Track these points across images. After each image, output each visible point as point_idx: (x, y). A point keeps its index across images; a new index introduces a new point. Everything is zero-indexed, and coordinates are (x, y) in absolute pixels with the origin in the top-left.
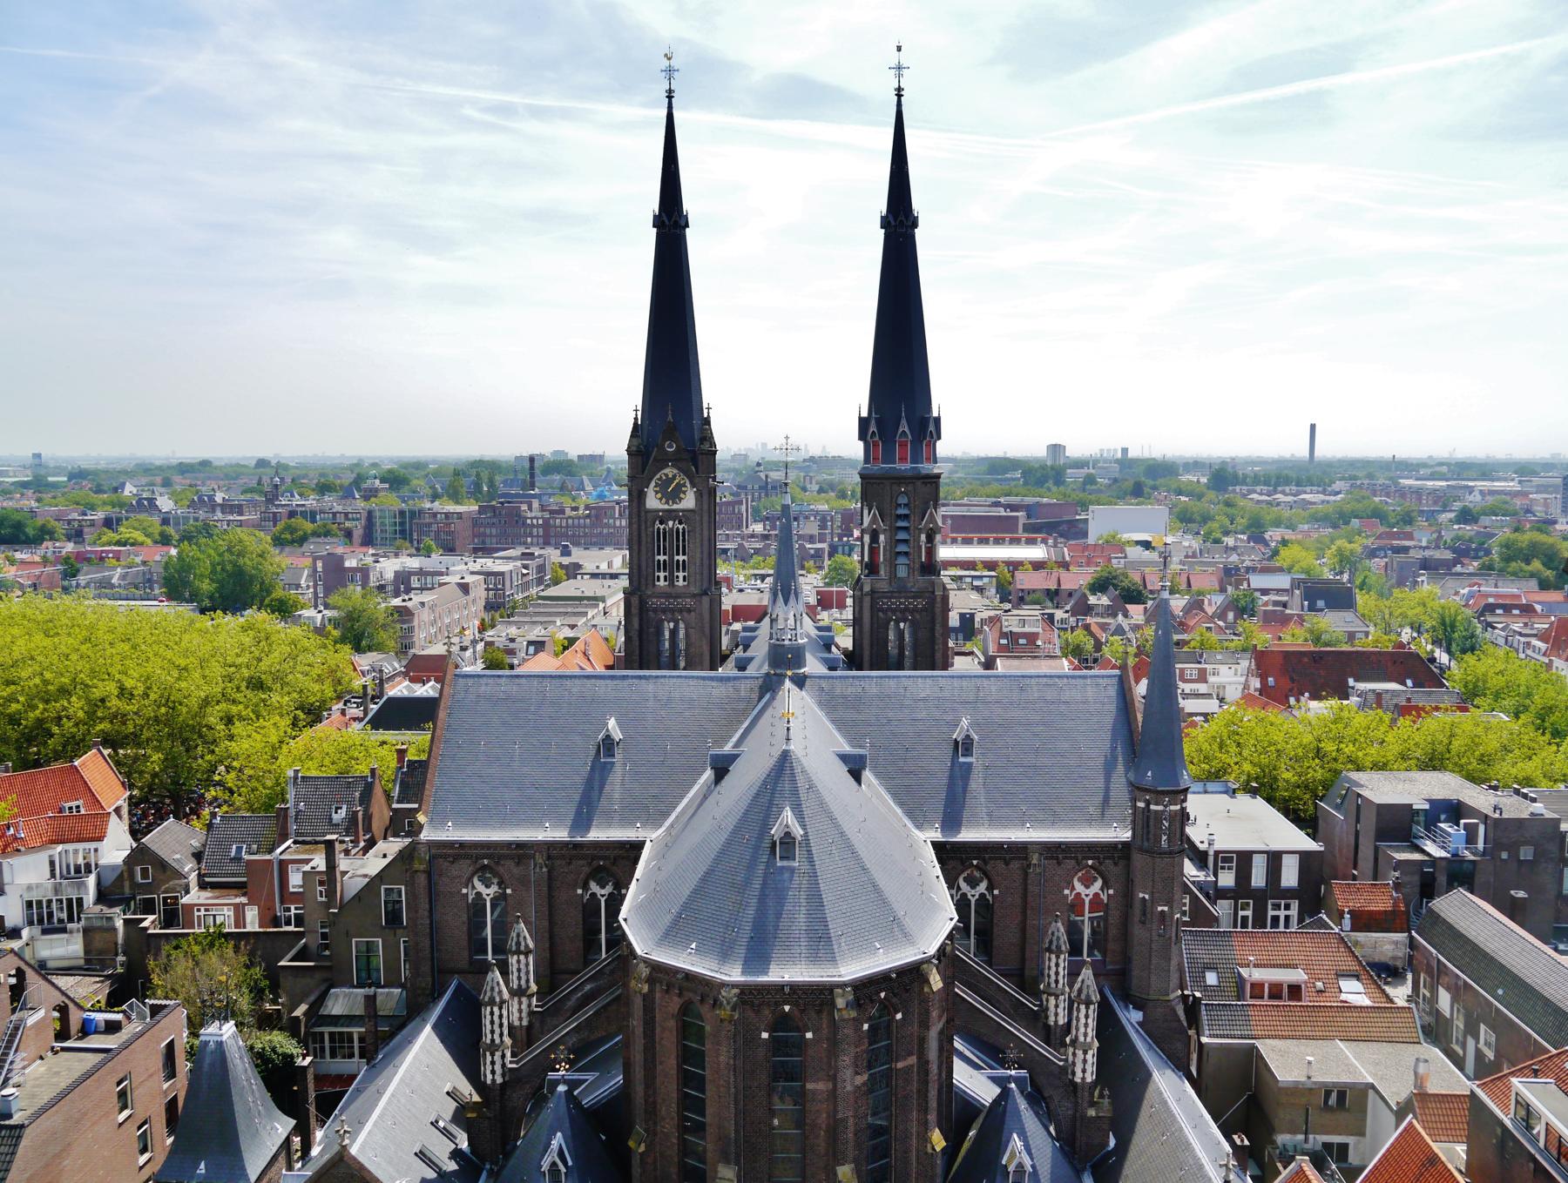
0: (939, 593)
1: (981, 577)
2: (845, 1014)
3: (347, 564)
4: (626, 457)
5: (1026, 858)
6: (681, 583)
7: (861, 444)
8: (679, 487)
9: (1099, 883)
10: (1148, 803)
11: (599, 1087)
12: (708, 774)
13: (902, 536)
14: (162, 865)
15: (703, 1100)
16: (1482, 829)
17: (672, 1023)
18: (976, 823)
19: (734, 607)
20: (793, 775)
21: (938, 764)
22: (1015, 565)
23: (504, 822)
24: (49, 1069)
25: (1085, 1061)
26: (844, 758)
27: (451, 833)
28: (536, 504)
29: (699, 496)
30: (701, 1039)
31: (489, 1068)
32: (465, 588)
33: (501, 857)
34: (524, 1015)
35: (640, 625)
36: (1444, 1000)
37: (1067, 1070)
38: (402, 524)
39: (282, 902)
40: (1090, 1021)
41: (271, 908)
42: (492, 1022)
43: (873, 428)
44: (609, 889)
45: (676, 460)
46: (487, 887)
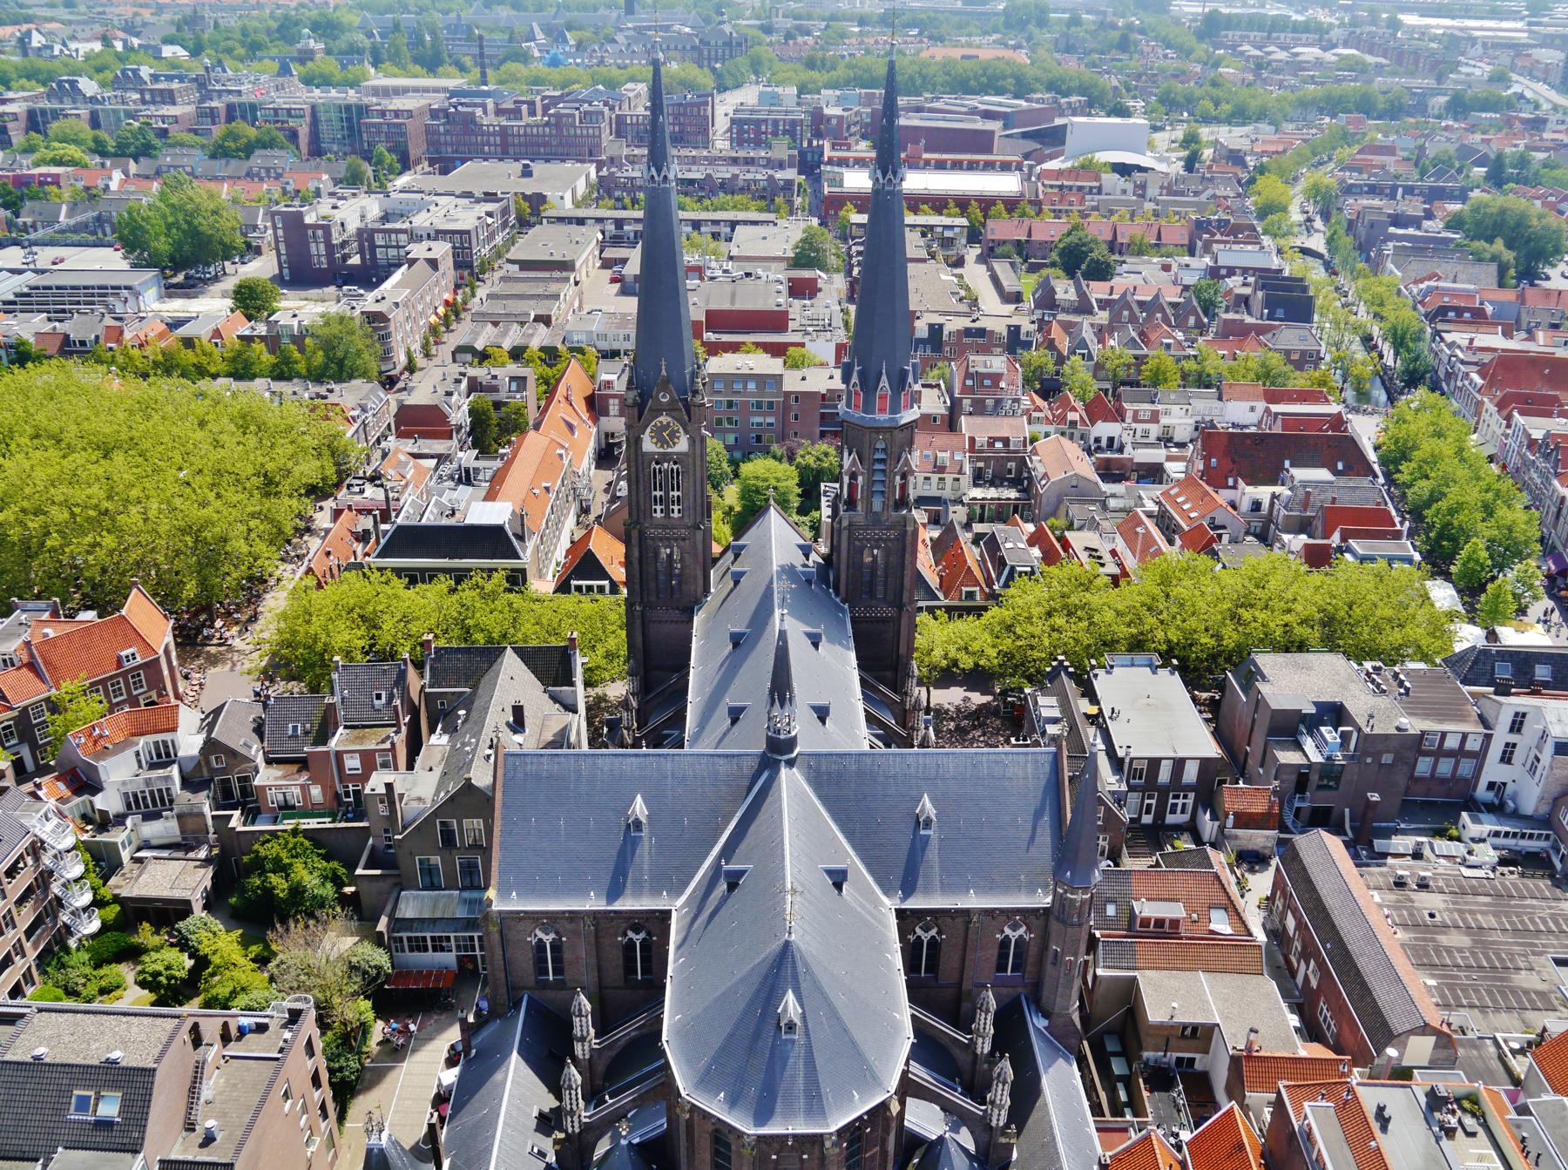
0: (910, 529)
1: (952, 227)
3: (309, 220)
6: (676, 515)
8: (673, 435)
13: (878, 477)
14: (232, 753)
16: (1355, 735)
18: (928, 891)
19: (709, 313)
20: (794, 962)
21: (904, 842)
22: (987, 203)
23: (557, 892)
24: (227, 1081)
26: (830, 872)
27: (515, 904)
28: (490, 102)
29: (692, 441)
32: (433, 264)
36: (1291, 923)
37: (986, 1117)
38: (349, 120)
39: (341, 781)
41: (333, 786)
44: (642, 935)
45: (670, 409)
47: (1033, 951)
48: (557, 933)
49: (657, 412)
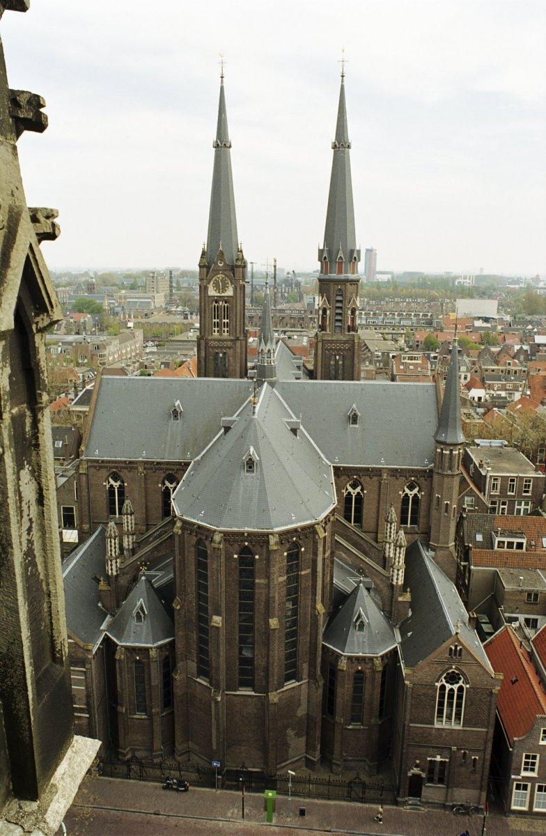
2: (275, 548)
4: (197, 269)
5: (380, 476)
7: (319, 263)
9: (417, 489)
10: (442, 450)
11: (161, 578)
12: (223, 430)
15: (207, 586)
17: (193, 549)
25: (398, 575)
29: (235, 290)
30: (206, 558)
31: (110, 567)
33: (121, 468)
34: (130, 543)
35: (205, 355)
40: (401, 555)
42: (111, 546)
43: (325, 255)
46: (116, 482)
47: (423, 506)
48: (123, 482)
49: (217, 271)
